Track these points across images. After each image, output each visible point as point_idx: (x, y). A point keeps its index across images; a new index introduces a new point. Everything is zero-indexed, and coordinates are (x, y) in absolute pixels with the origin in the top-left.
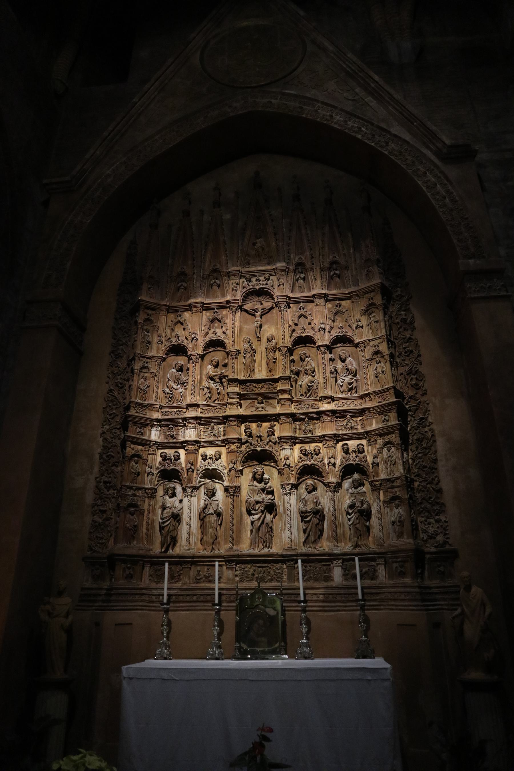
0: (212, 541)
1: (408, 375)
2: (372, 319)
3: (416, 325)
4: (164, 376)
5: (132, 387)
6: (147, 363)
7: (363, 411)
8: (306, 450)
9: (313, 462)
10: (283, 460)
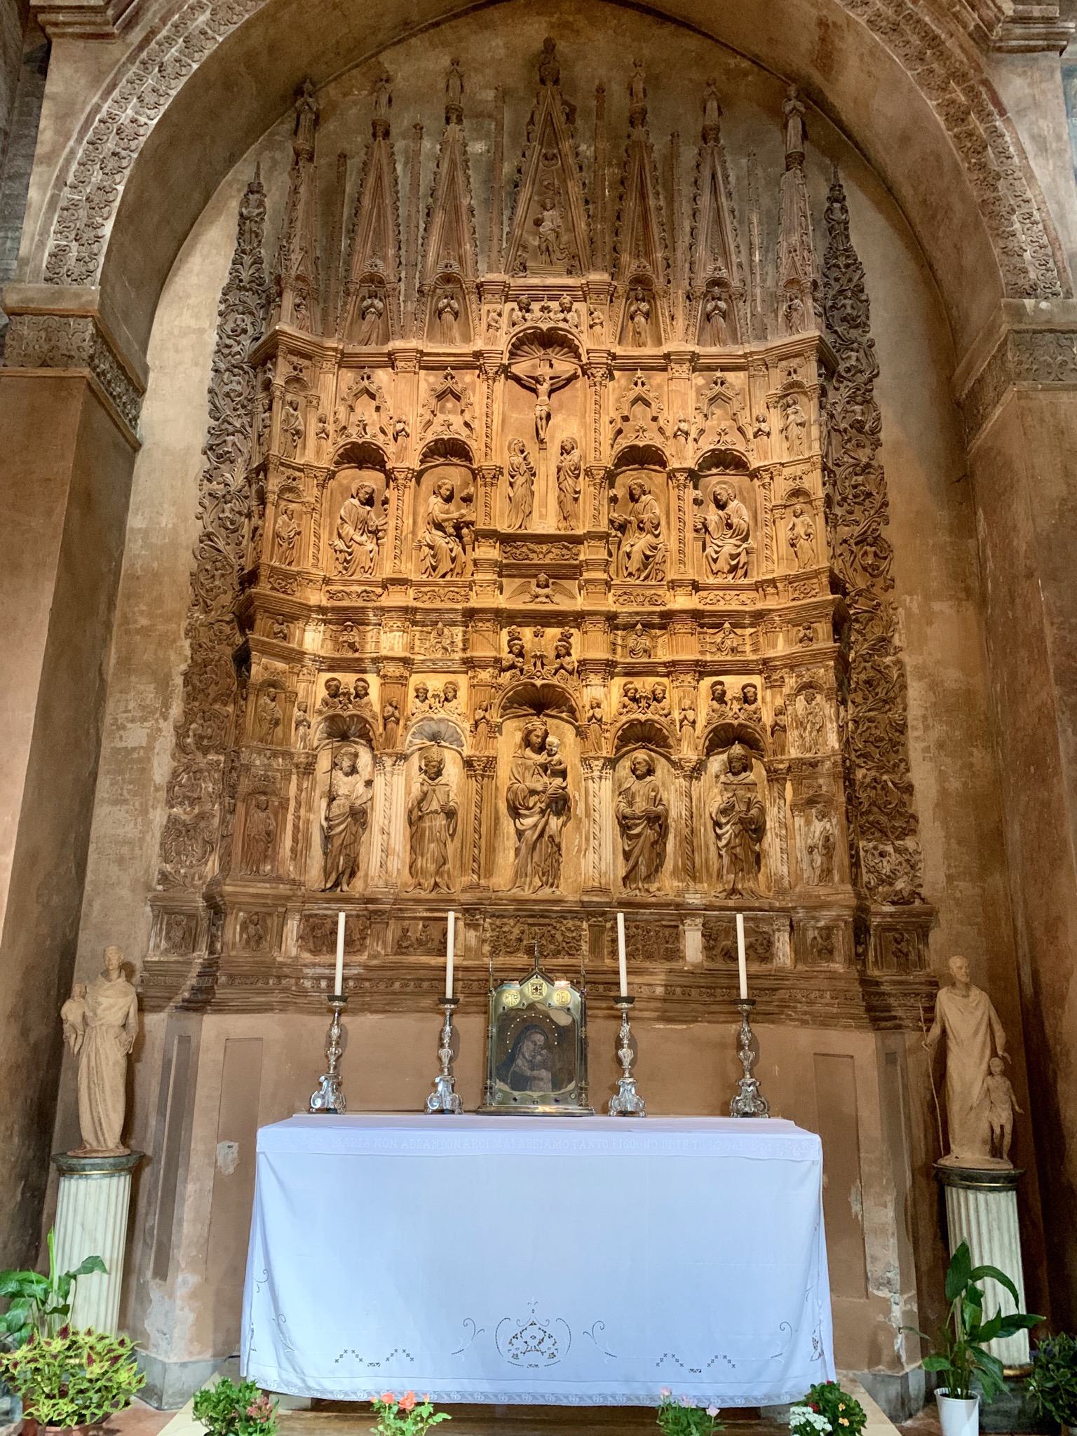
0: (432, 867)
1: (857, 544)
2: (792, 417)
3: (882, 435)
4: (331, 513)
5: (260, 531)
6: (294, 479)
7: (759, 617)
8: (636, 690)
9: (649, 716)
10: (588, 707)
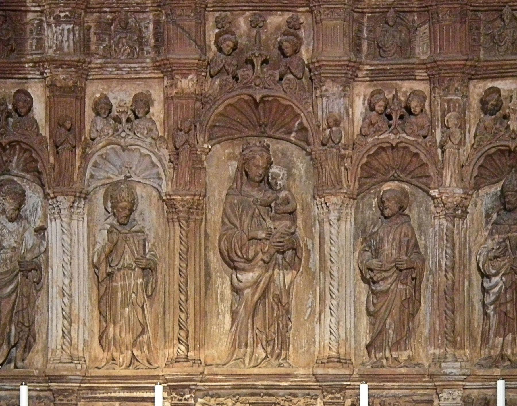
0: (128, 338)
